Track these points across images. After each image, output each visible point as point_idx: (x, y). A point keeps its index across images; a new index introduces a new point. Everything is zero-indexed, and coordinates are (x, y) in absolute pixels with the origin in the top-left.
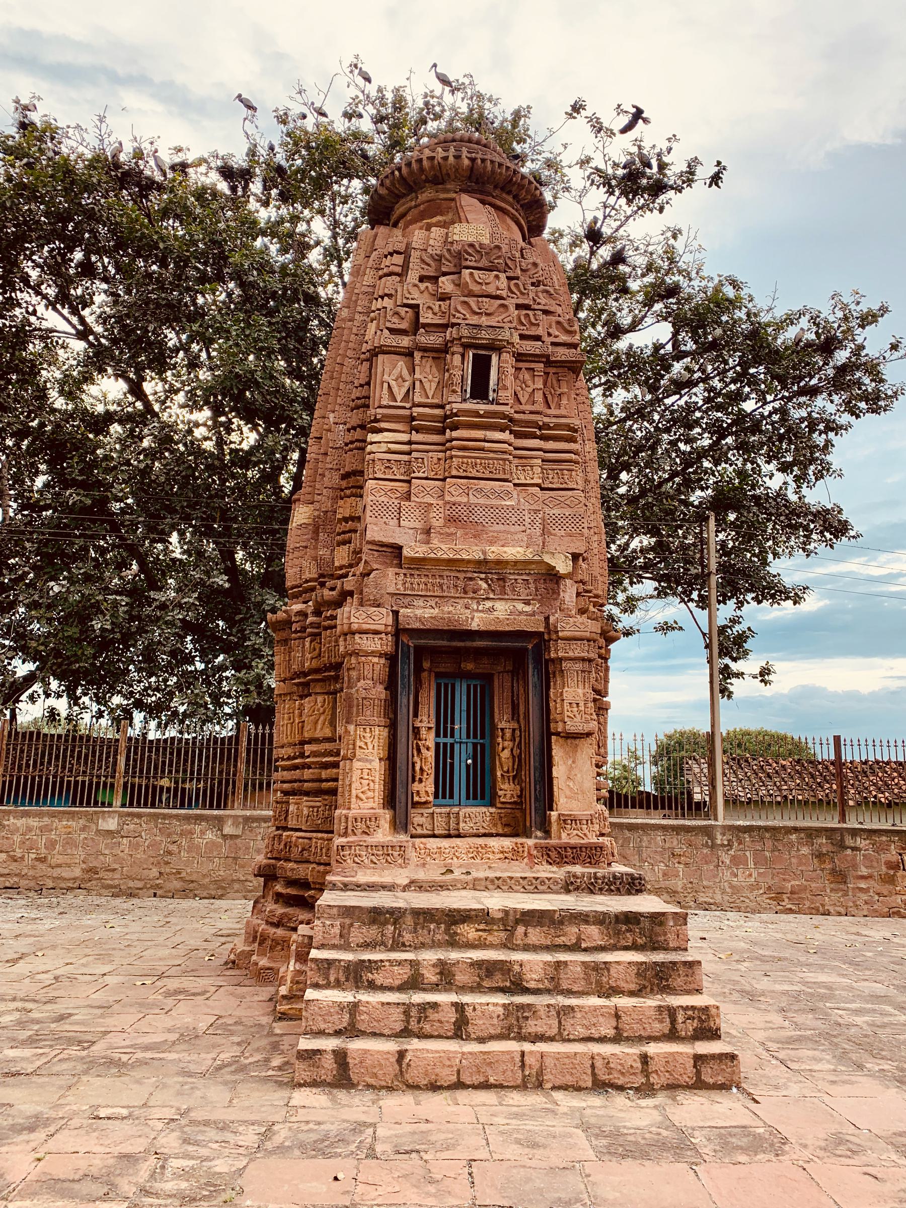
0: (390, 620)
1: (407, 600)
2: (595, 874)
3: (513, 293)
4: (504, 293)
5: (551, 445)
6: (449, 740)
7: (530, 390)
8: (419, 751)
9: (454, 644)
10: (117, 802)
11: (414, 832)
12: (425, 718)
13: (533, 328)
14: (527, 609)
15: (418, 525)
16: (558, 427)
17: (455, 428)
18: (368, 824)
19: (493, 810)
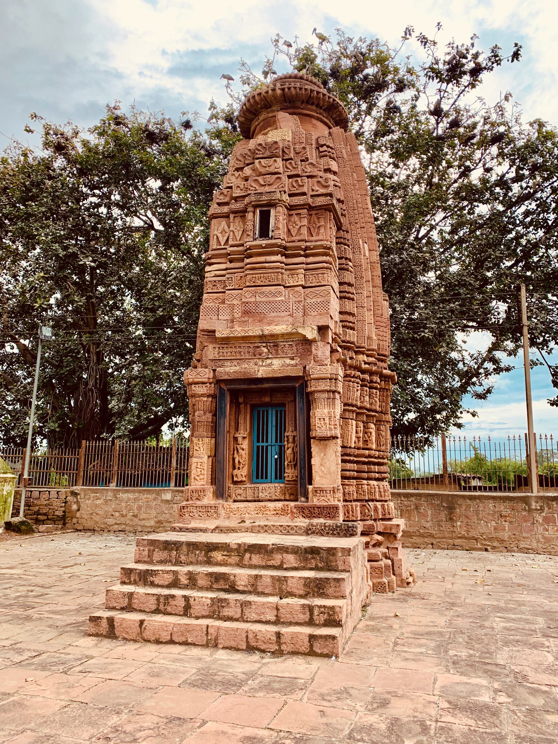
0: (211, 375)
1: (220, 363)
2: (325, 523)
3: (288, 168)
4: (281, 170)
5: (311, 259)
6: (265, 444)
7: (298, 227)
8: (238, 450)
9: (251, 387)
10: (173, 484)
11: (236, 498)
12: (242, 432)
13: (301, 188)
14: (293, 362)
15: (228, 318)
16: (315, 247)
17: (249, 256)
18: (200, 493)
19: (282, 485)
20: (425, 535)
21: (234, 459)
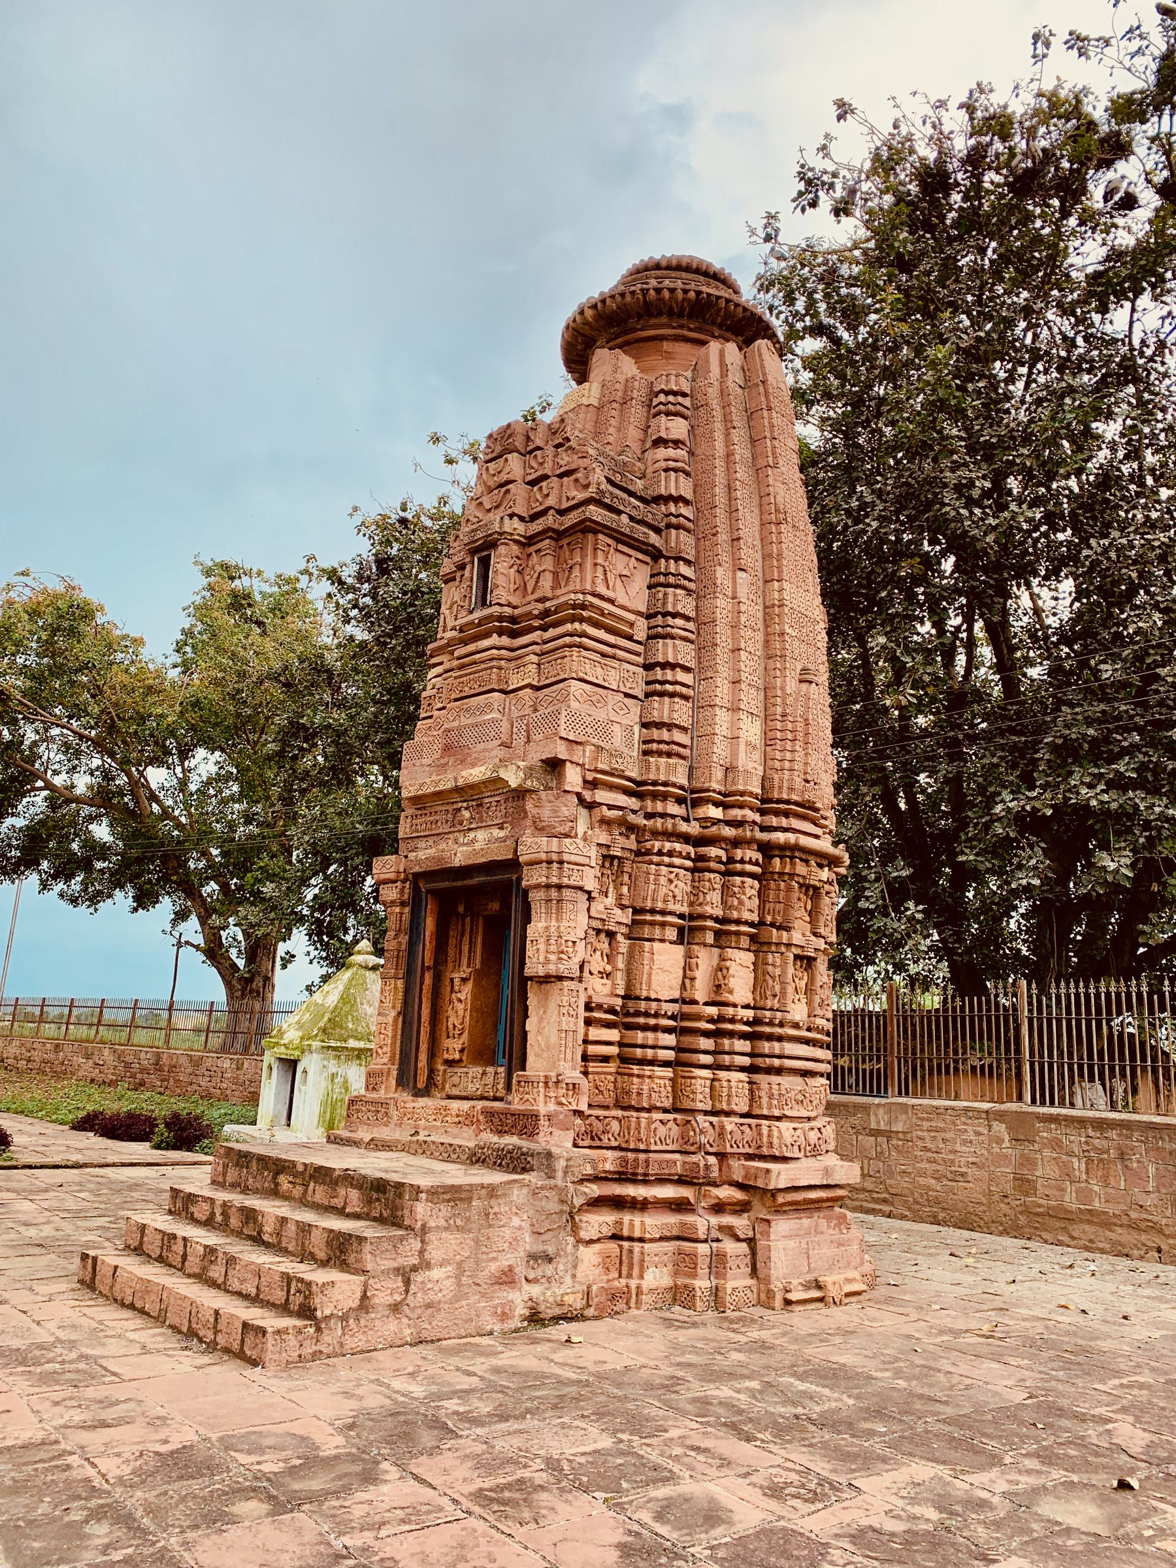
5: (552, 632)
14: (502, 834)
20: (1143, 1225)
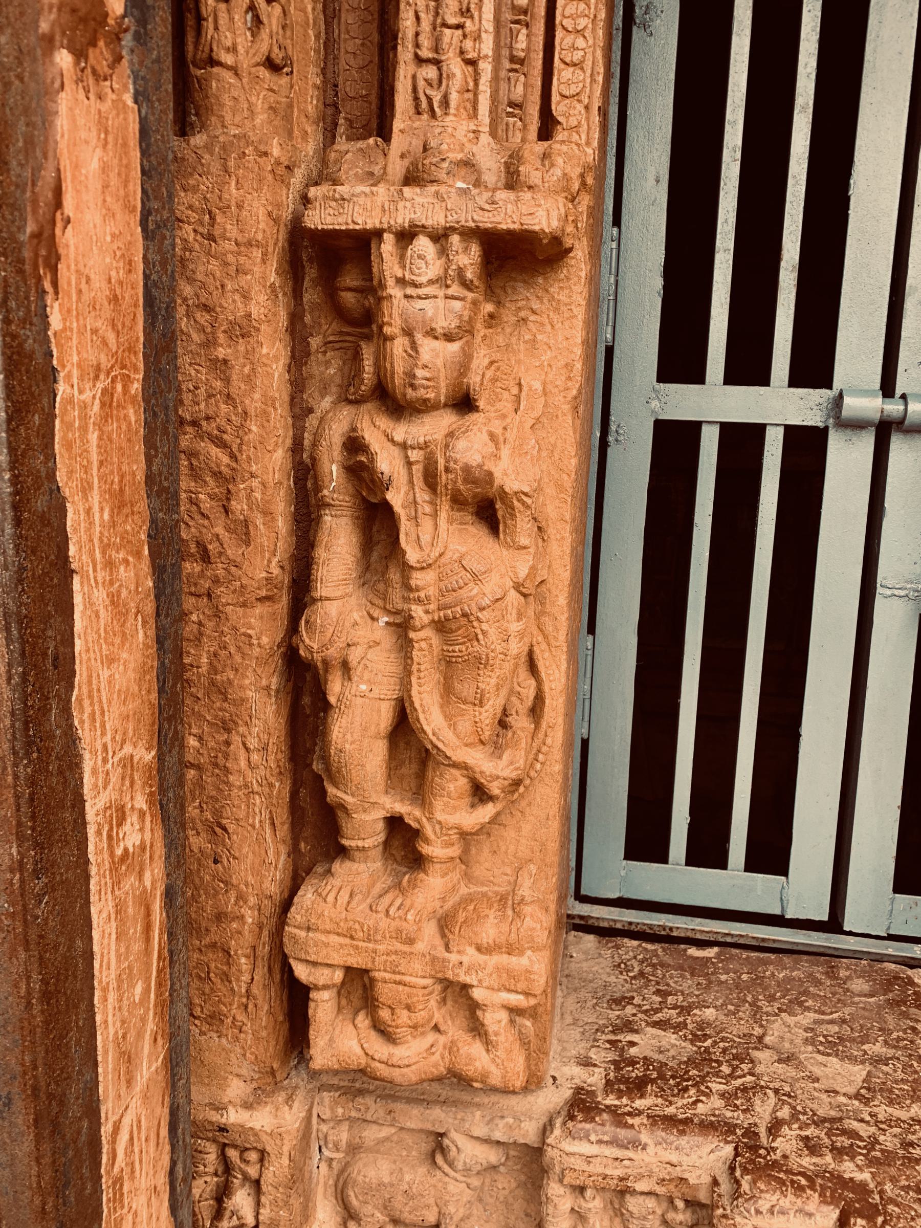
6: (779, 405)
8: (377, 522)
12: (462, 134)
21: (306, 690)
